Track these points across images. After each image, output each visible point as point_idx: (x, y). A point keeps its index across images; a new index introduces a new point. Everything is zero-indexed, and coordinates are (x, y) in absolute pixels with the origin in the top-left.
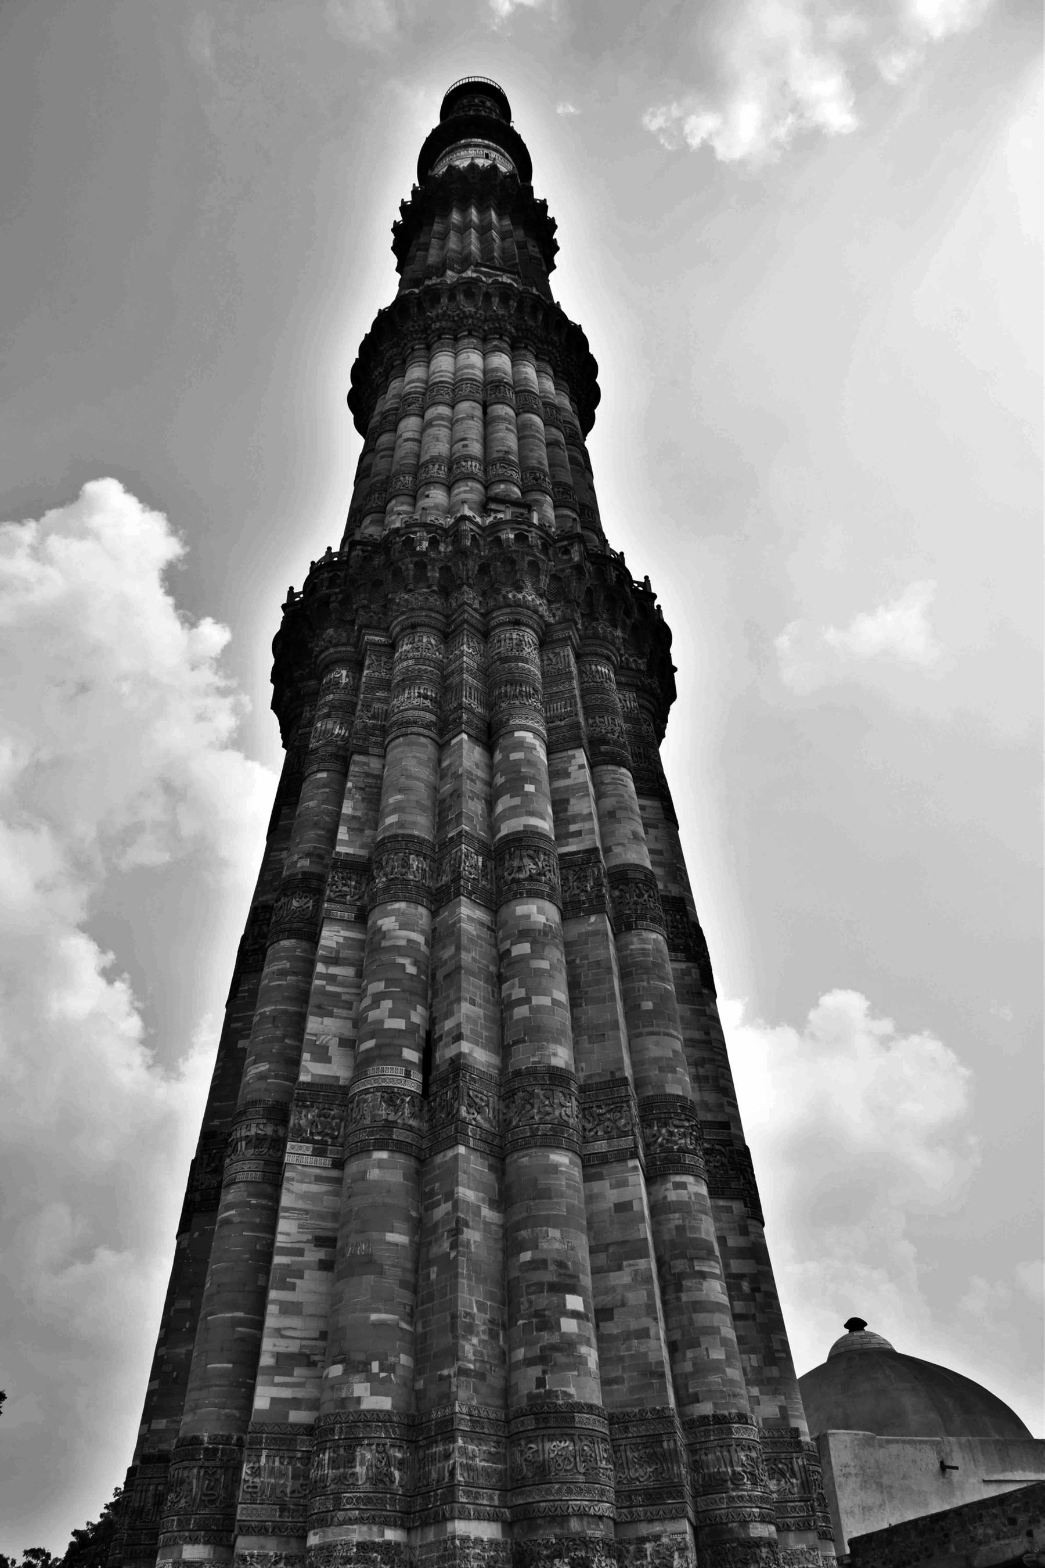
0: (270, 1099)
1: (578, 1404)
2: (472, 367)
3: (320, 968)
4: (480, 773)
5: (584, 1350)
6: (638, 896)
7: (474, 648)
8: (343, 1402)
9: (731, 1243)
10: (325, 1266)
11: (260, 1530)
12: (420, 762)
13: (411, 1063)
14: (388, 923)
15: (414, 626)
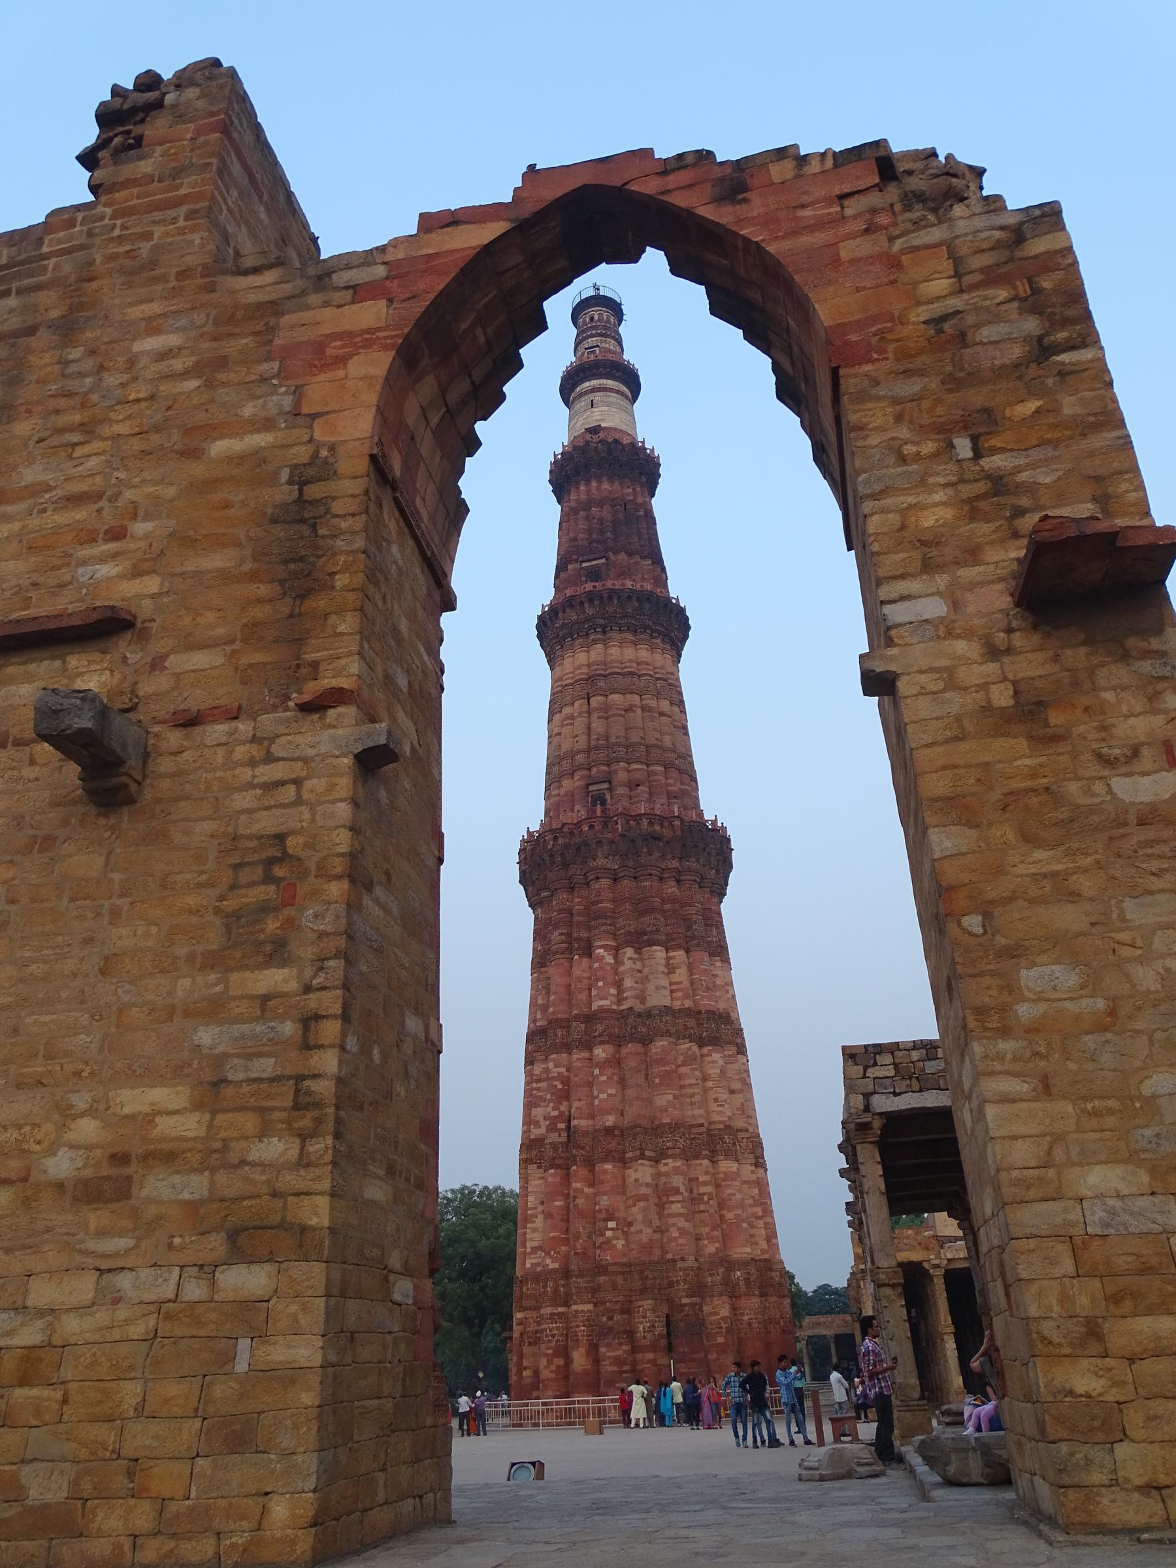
4: (586, 975)
14: (551, 1065)
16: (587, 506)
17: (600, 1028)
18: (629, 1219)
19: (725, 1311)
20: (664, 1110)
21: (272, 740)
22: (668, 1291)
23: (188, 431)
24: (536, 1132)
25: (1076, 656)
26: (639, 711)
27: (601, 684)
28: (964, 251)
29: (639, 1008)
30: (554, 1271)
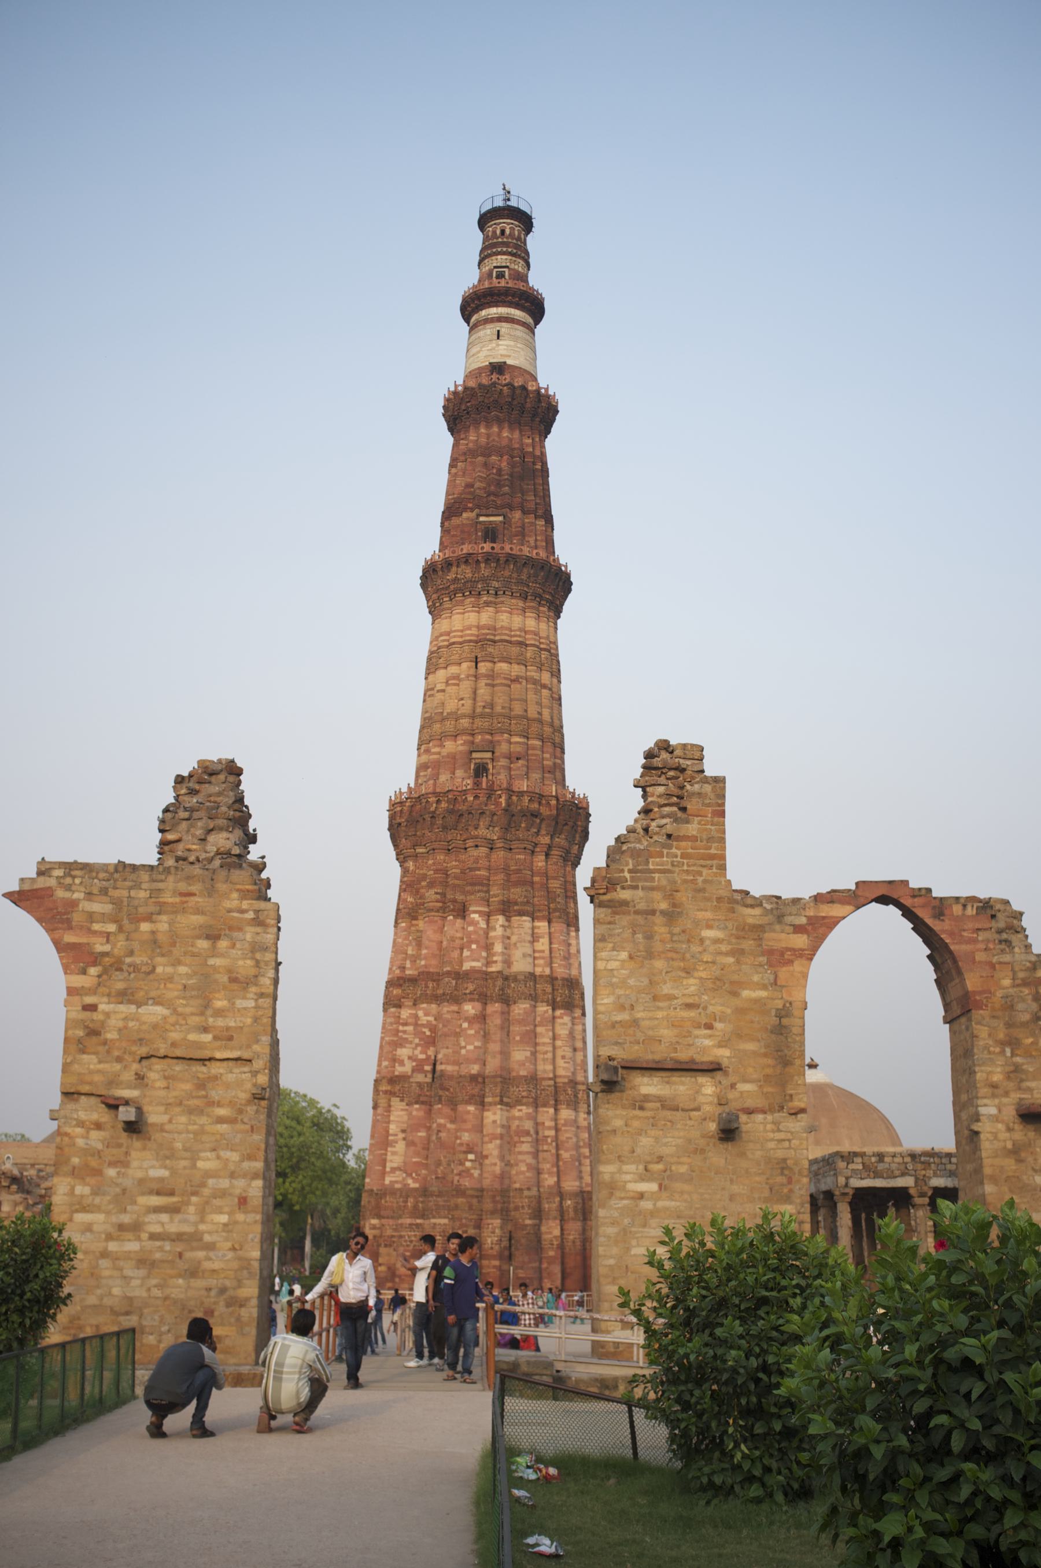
4: (459, 935)
8: (405, 1185)
10: (404, 1139)
11: (388, 1218)
14: (420, 1013)
16: (486, 451)
17: (471, 987)
18: (484, 1153)
19: (557, 1232)
20: (522, 1064)
21: (780, 1123)
22: (513, 1213)
23: (732, 983)
24: (399, 1070)
25: (1031, 1134)
27: (490, 649)
28: (1017, 969)
29: (506, 972)
30: (416, 1190)
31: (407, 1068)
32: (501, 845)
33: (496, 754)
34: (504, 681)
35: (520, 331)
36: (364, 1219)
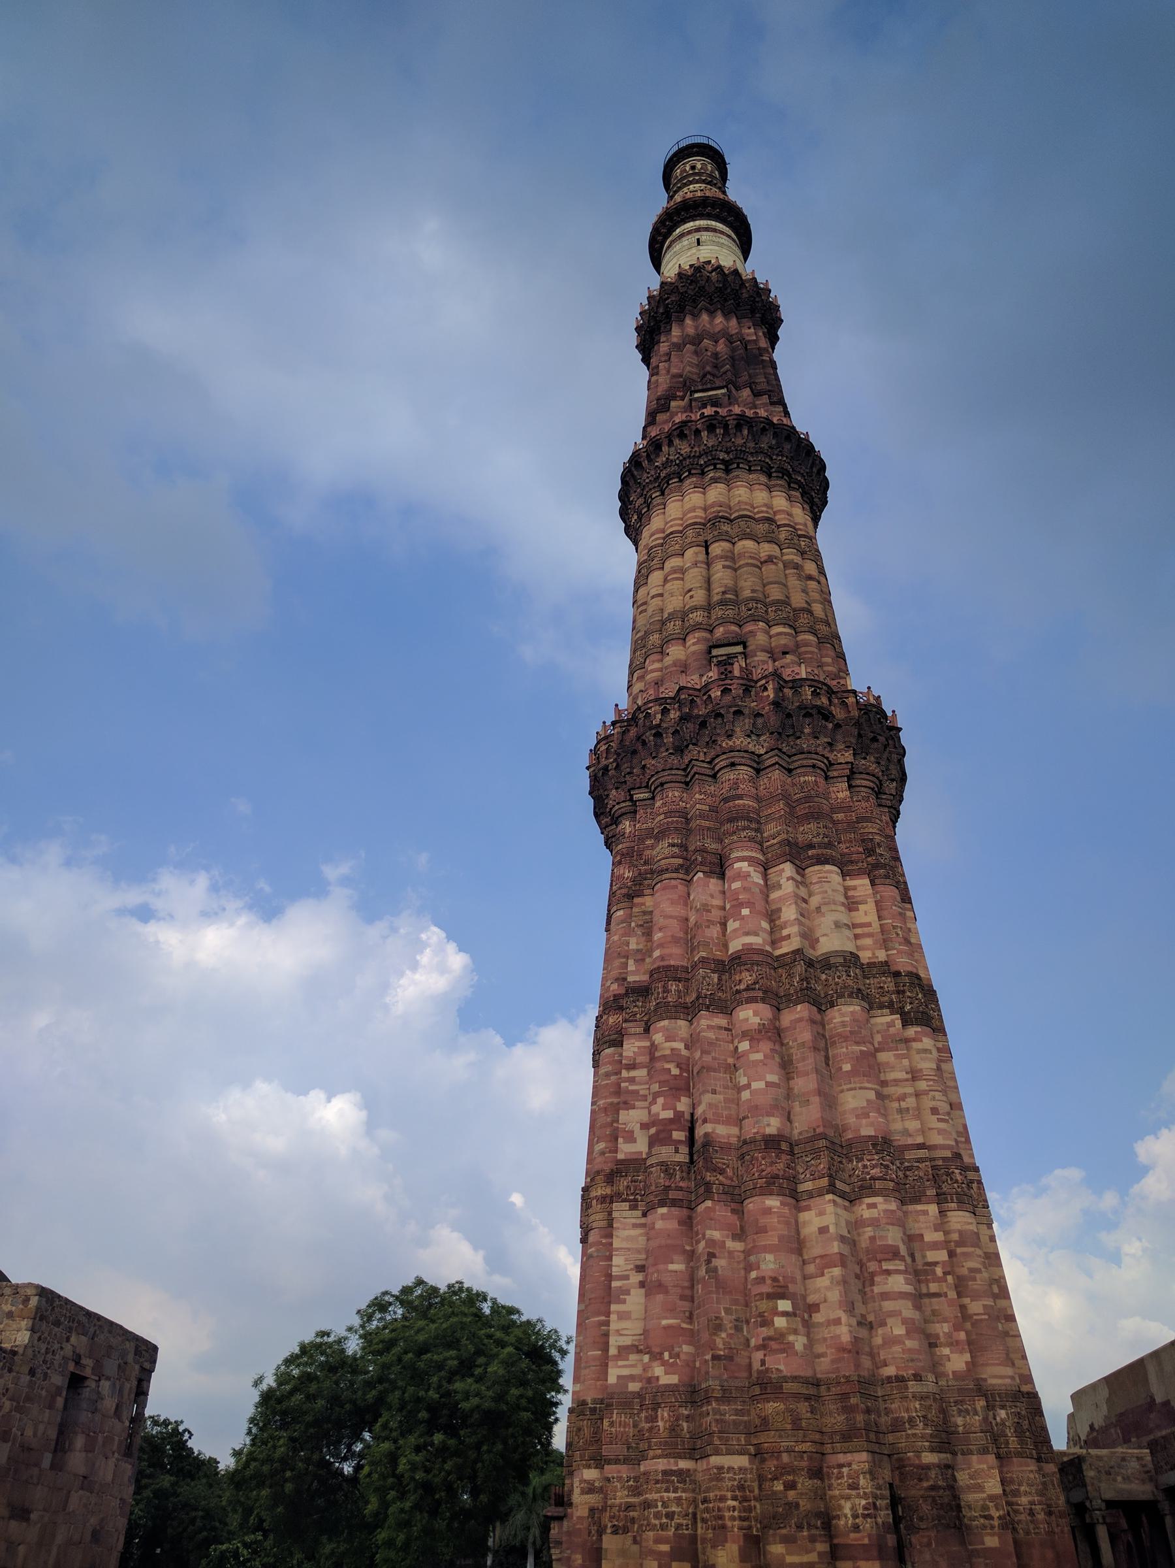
0: (607, 1168)
1: (784, 1377)
2: (693, 509)
3: (624, 1074)
4: (717, 902)
5: (791, 1338)
6: (839, 977)
7: (705, 793)
8: (649, 1380)
9: (927, 1238)
10: (642, 1284)
11: (617, 1461)
12: (673, 902)
13: (680, 1142)
14: (658, 1038)
15: (662, 784)
17: (747, 978)
18: (811, 1299)
19: (993, 1486)
22: (891, 1438)
24: (625, 1149)
26: (781, 565)
31: (640, 1146)
32: (773, 761)
33: (750, 648)
34: (750, 561)
35: (724, 240)
36: (571, 1474)
